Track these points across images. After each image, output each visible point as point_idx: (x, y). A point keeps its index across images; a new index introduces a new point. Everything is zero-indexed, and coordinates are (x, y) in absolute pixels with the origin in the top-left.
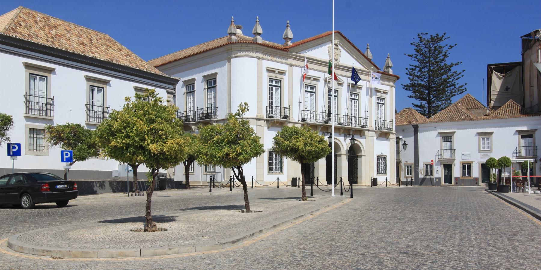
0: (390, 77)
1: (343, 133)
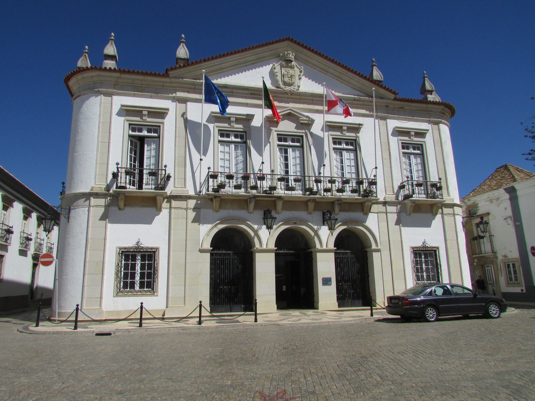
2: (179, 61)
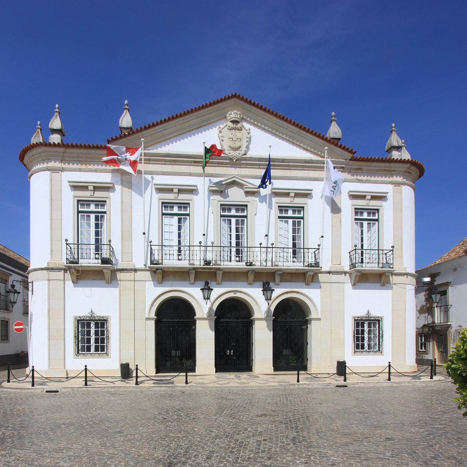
0: (392, 165)
1: (254, 281)
2: (123, 130)
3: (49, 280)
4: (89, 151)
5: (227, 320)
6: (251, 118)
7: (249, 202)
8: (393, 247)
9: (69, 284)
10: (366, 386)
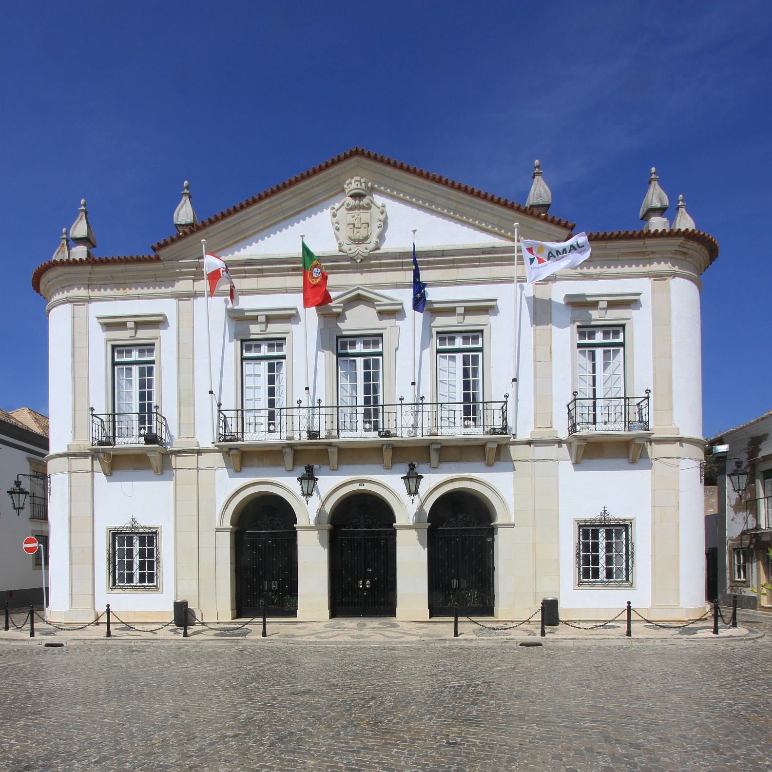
0: (648, 242)
1: (393, 462)
3: (70, 472)
4: (127, 268)
5: (352, 529)
6: (386, 187)
7: (386, 329)
8: (648, 391)
9: (100, 476)
10: (577, 644)
